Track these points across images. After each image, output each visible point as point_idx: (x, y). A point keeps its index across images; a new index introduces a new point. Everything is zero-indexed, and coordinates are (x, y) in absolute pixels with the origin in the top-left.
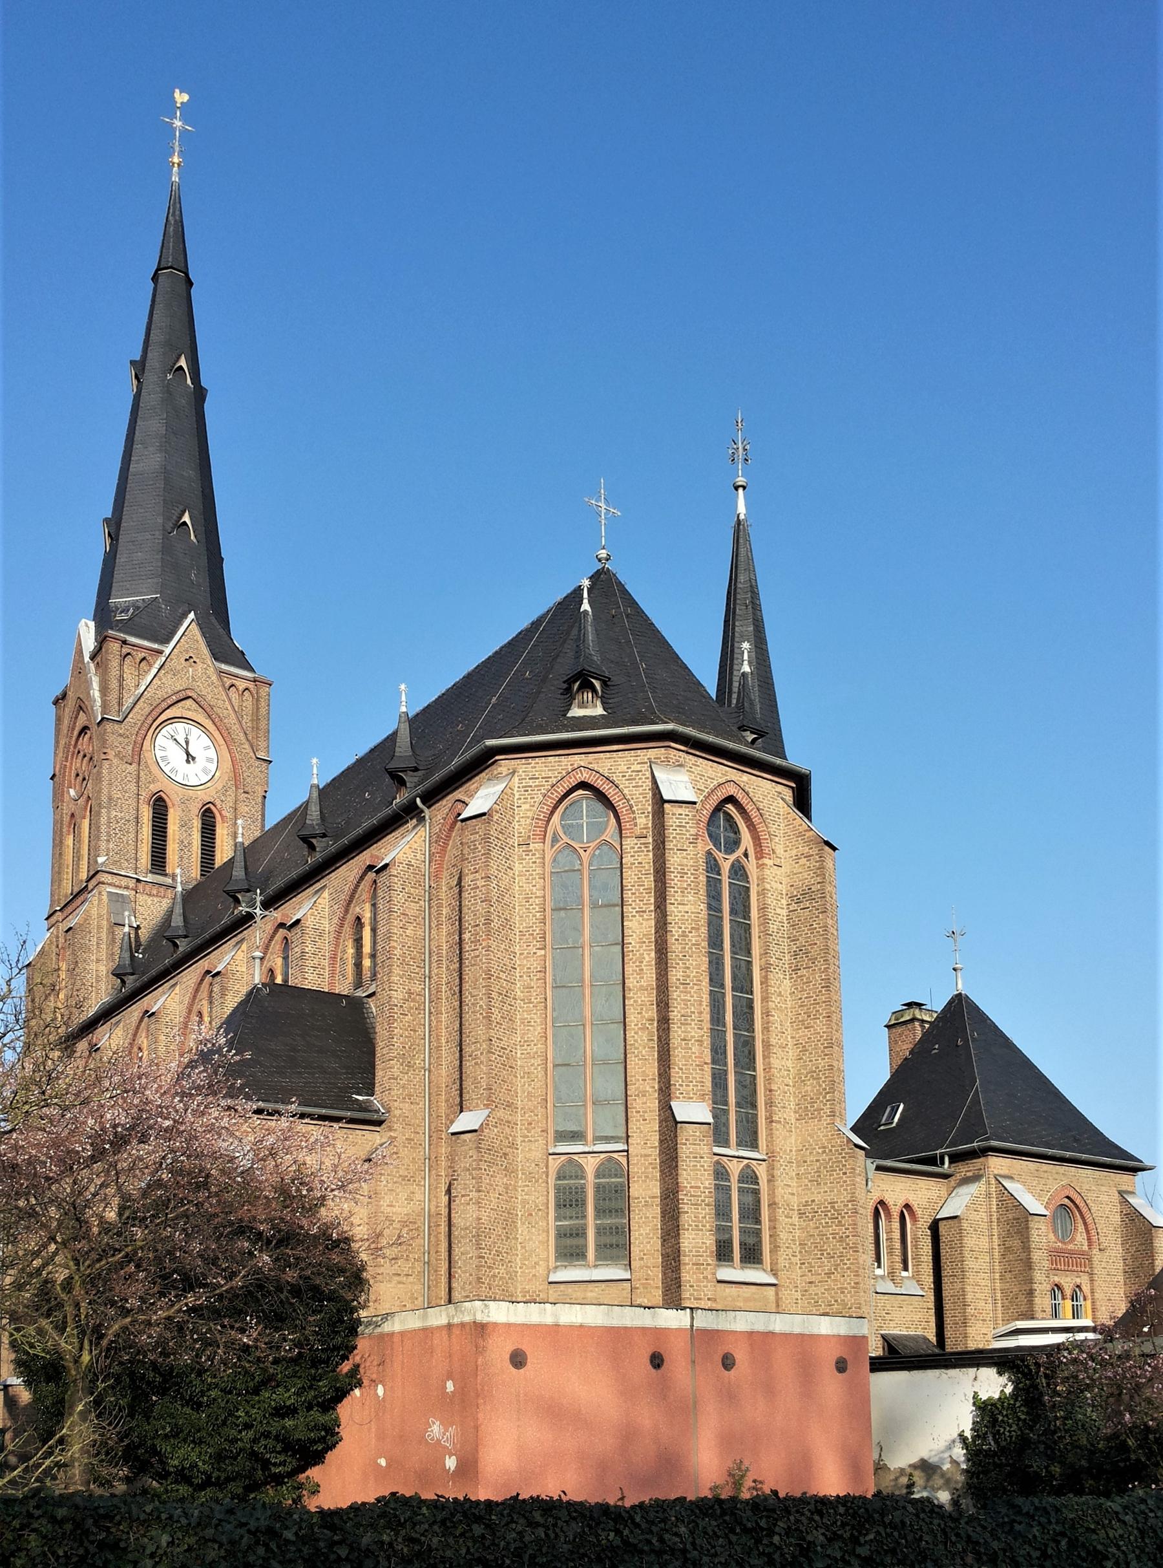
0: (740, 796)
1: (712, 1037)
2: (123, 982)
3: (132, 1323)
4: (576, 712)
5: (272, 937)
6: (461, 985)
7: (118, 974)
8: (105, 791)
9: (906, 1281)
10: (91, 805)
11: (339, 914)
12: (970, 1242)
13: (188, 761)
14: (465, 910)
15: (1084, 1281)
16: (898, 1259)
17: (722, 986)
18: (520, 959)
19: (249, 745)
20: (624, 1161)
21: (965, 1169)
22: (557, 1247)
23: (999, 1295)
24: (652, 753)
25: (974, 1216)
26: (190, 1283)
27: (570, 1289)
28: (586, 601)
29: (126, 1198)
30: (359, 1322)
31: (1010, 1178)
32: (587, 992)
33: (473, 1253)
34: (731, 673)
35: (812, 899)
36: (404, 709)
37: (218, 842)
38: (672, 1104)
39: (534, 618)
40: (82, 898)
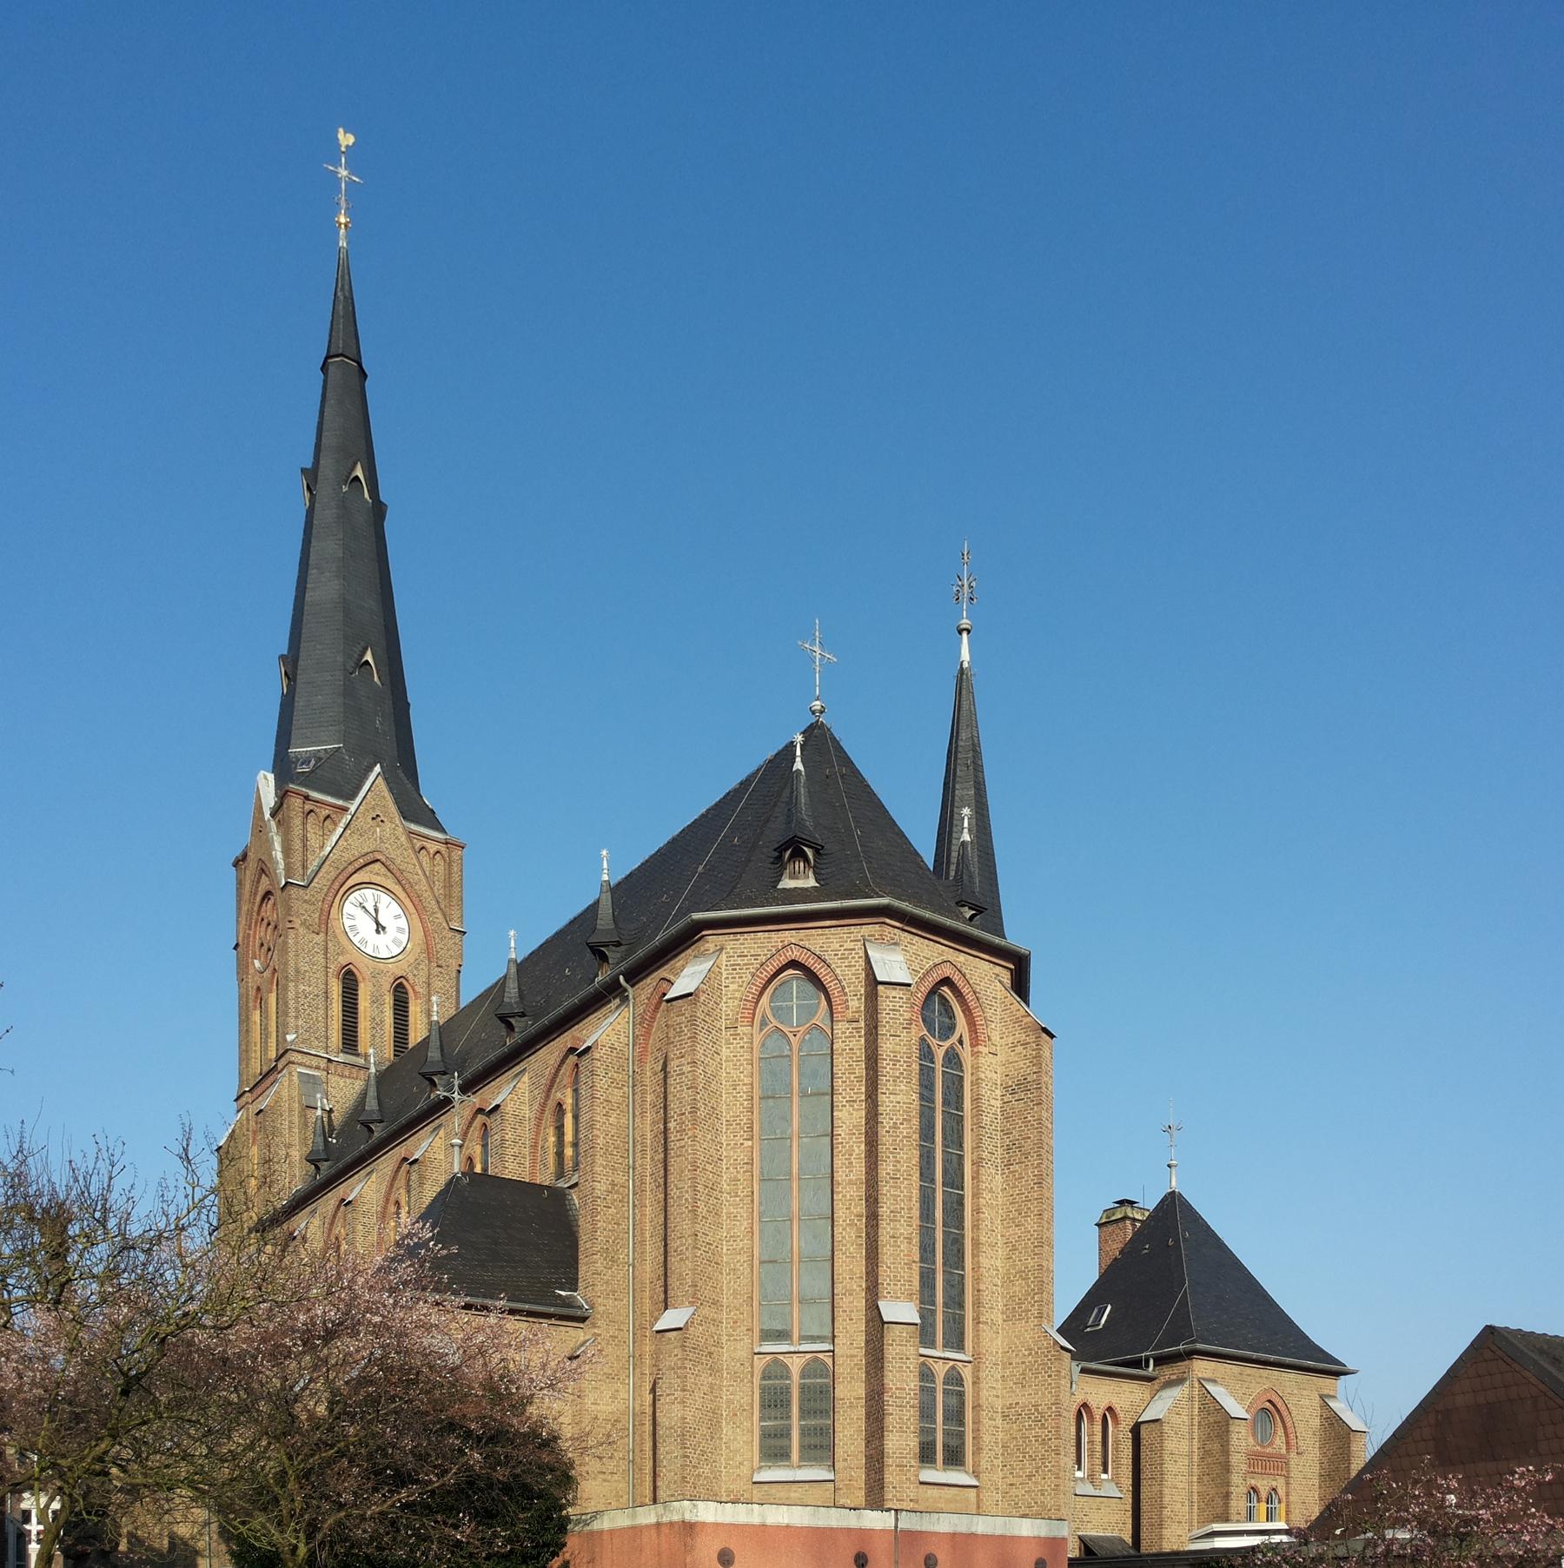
0: (956, 978)
1: (921, 1235)
2: (317, 1168)
3: (348, 1516)
4: (787, 883)
5: (470, 1124)
6: (666, 1176)
7: (313, 1160)
8: (292, 963)
9: (1106, 1484)
10: (278, 978)
11: (540, 1099)
12: (1170, 1445)
13: (378, 932)
14: (670, 1097)
15: (1280, 1484)
16: (1099, 1462)
17: (933, 1181)
18: (726, 1146)
19: (439, 911)
20: (829, 1362)
21: (1169, 1372)
22: (761, 1447)
23: (1196, 1498)
24: (866, 930)
25: (1175, 1419)
26: (403, 1479)
27: (774, 1489)
28: (798, 759)
29: (335, 1392)
30: (568, 1519)
31: (1214, 1381)
32: (795, 1185)
33: (678, 1452)
34: (950, 842)
35: (1027, 1089)
36: (606, 877)
37: (411, 1019)
38: (881, 1304)
39: (743, 777)
40: (271, 1078)
